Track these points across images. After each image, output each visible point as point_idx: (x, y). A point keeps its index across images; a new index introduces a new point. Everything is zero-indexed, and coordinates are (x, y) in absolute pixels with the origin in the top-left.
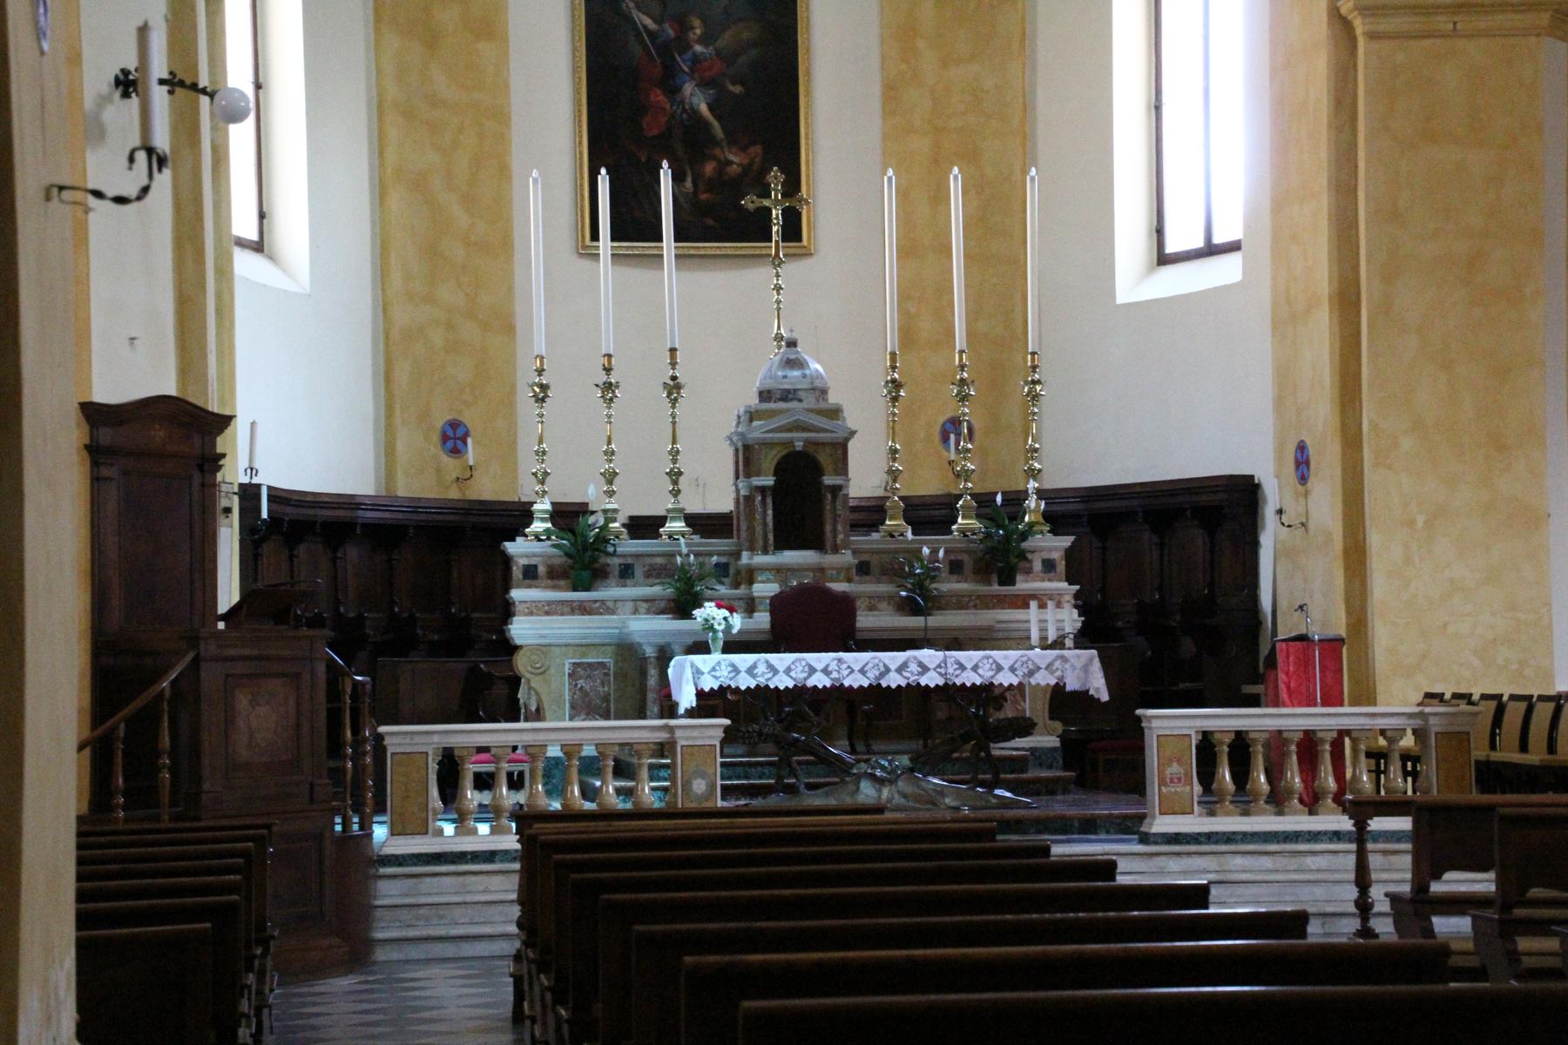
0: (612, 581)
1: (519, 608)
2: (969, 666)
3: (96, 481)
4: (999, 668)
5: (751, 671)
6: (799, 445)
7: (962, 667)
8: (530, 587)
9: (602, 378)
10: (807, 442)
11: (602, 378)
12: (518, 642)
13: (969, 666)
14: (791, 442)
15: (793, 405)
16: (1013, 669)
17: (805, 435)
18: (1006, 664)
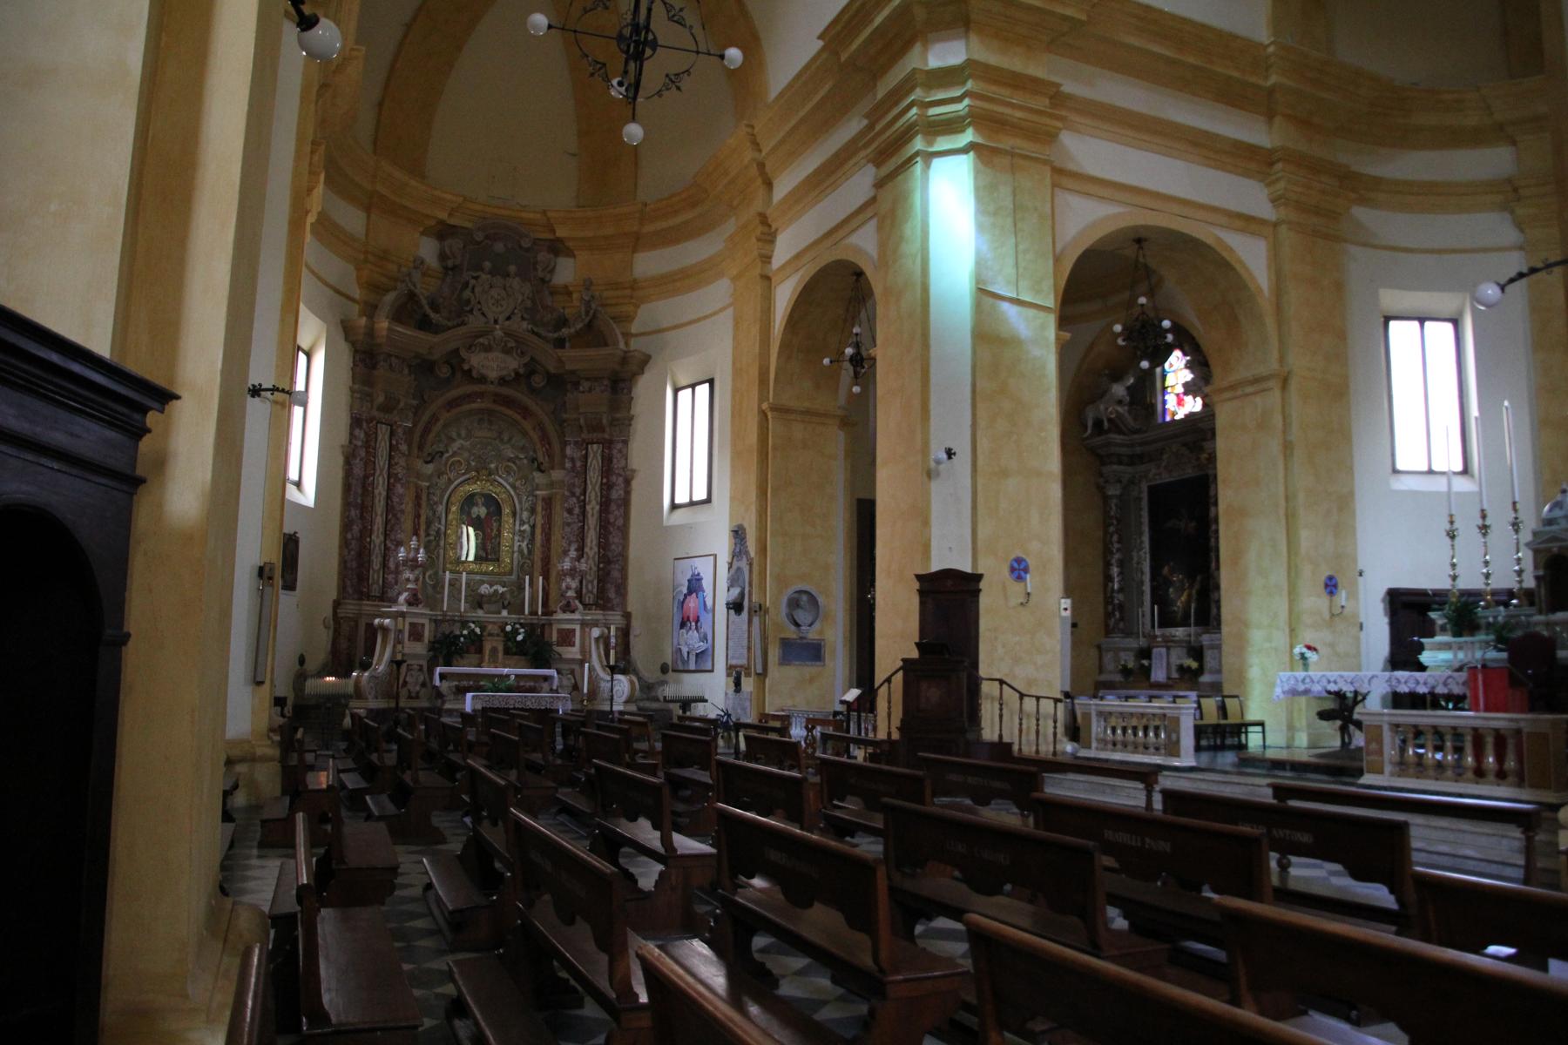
0: (1483, 632)
1: (1426, 646)
2: (1403, 680)
3: (922, 603)
4: (1418, 683)
5: (1303, 681)
6: (1555, 550)
7: (1399, 681)
8: (1442, 635)
9: (1480, 522)
10: (1560, 548)
11: (1480, 522)
12: (1426, 664)
13: (1403, 680)
14: (1549, 550)
15: (1554, 528)
16: (1425, 684)
17: (1559, 544)
18: (1422, 681)
